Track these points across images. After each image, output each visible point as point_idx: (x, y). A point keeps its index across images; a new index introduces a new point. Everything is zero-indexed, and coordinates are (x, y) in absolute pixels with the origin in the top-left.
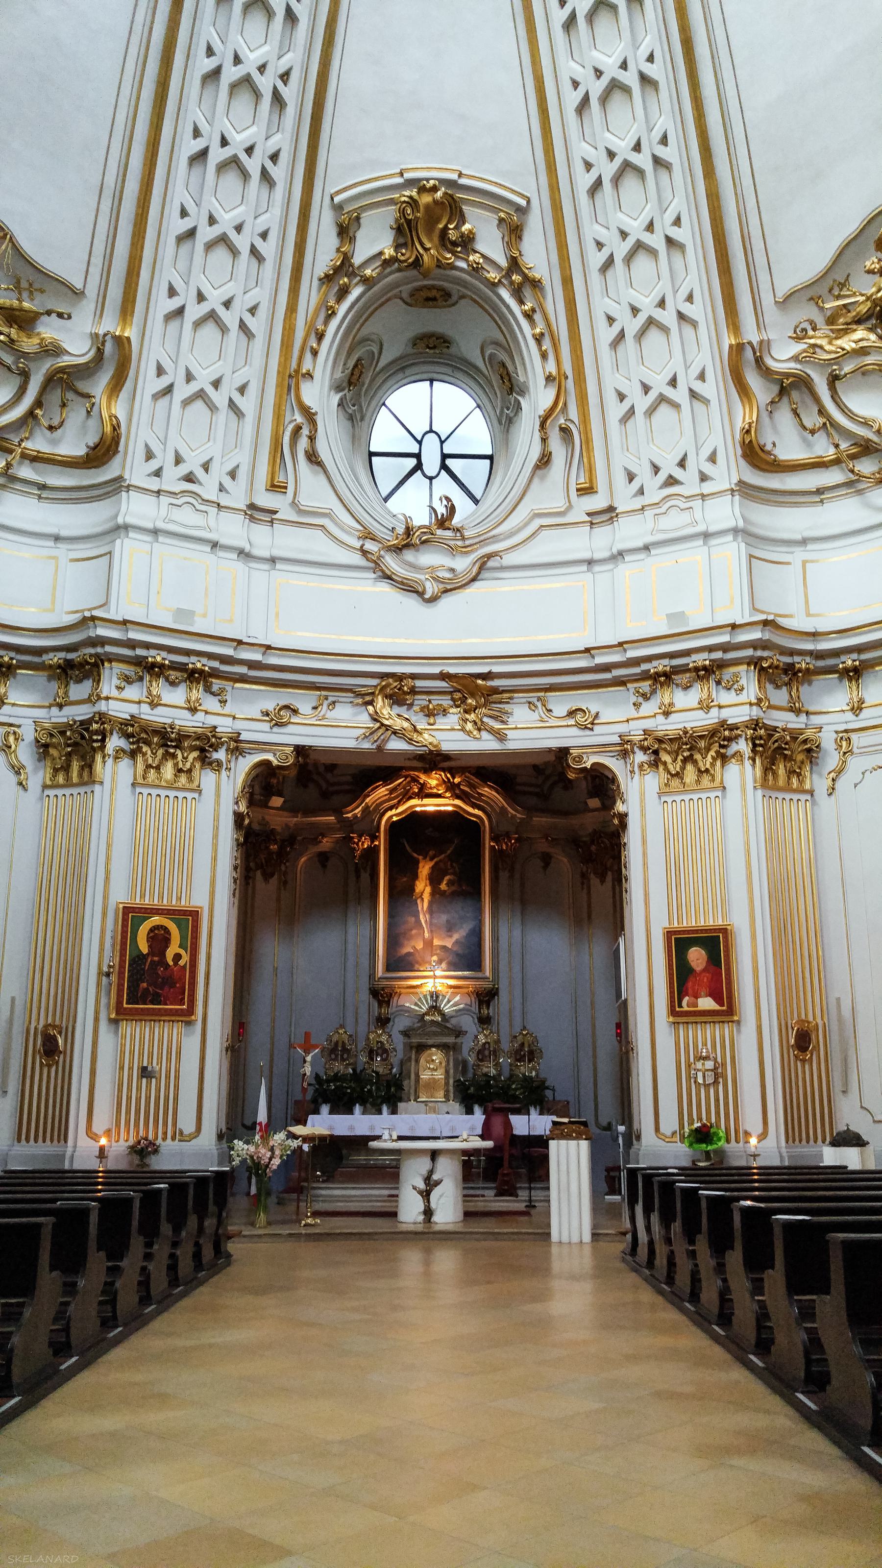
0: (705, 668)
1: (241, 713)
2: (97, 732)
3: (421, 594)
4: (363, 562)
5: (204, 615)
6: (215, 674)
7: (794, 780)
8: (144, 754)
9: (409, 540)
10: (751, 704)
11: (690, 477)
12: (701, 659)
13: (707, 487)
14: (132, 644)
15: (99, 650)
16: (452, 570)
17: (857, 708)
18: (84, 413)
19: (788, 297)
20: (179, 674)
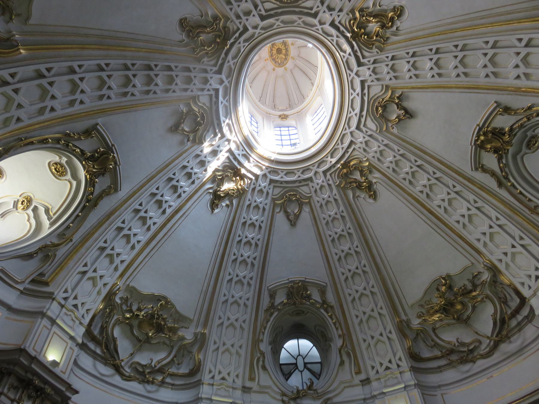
18: (189, 358)
19: (412, 306)
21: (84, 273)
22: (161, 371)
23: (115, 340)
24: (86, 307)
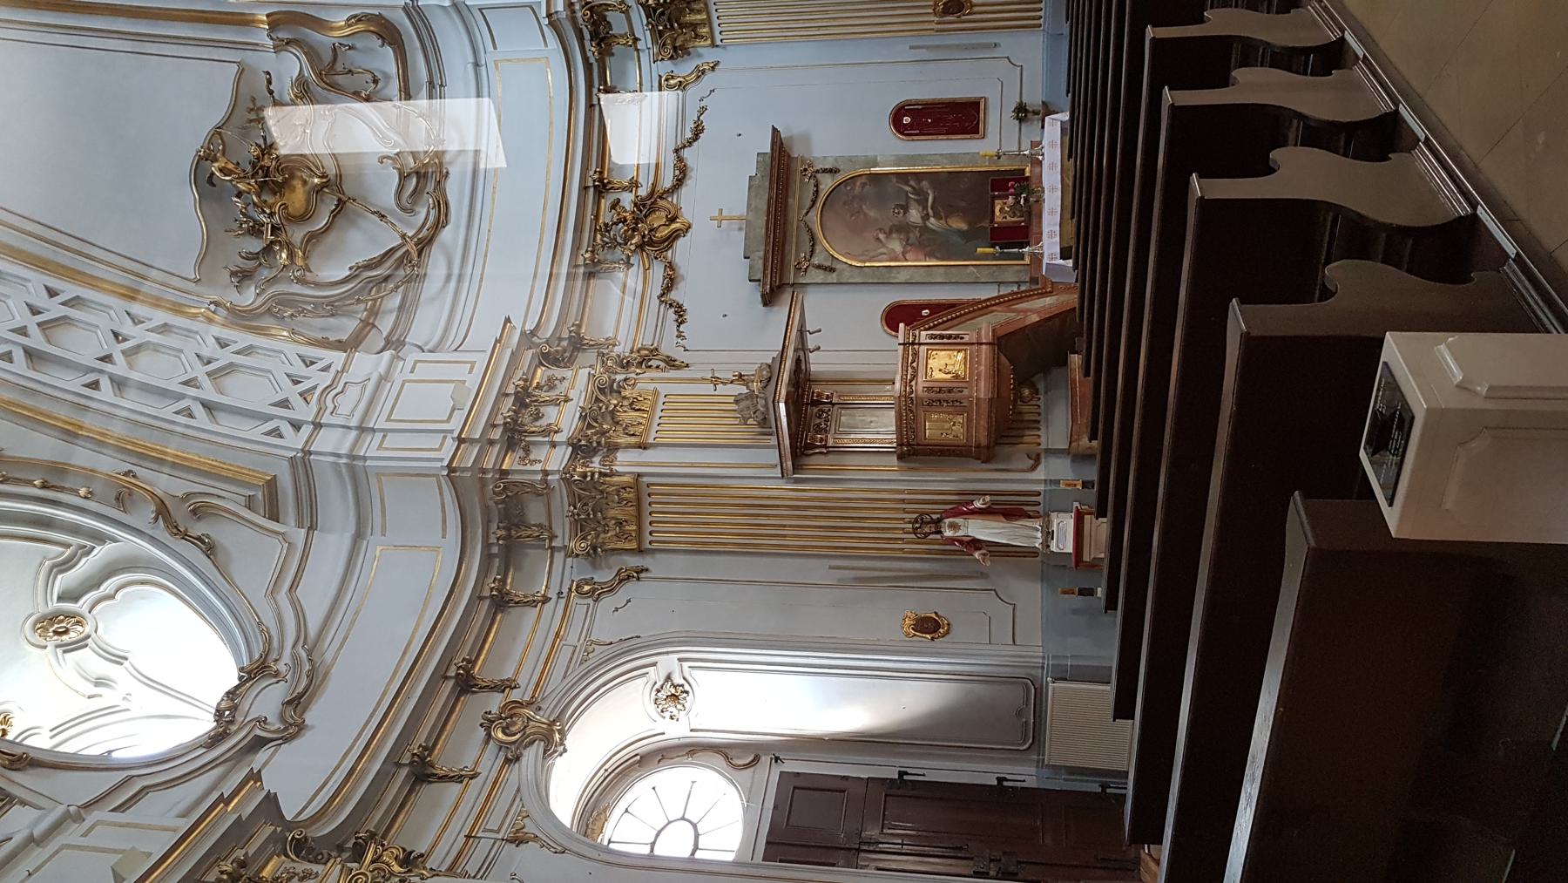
21: (208, 407)
24: (299, 369)
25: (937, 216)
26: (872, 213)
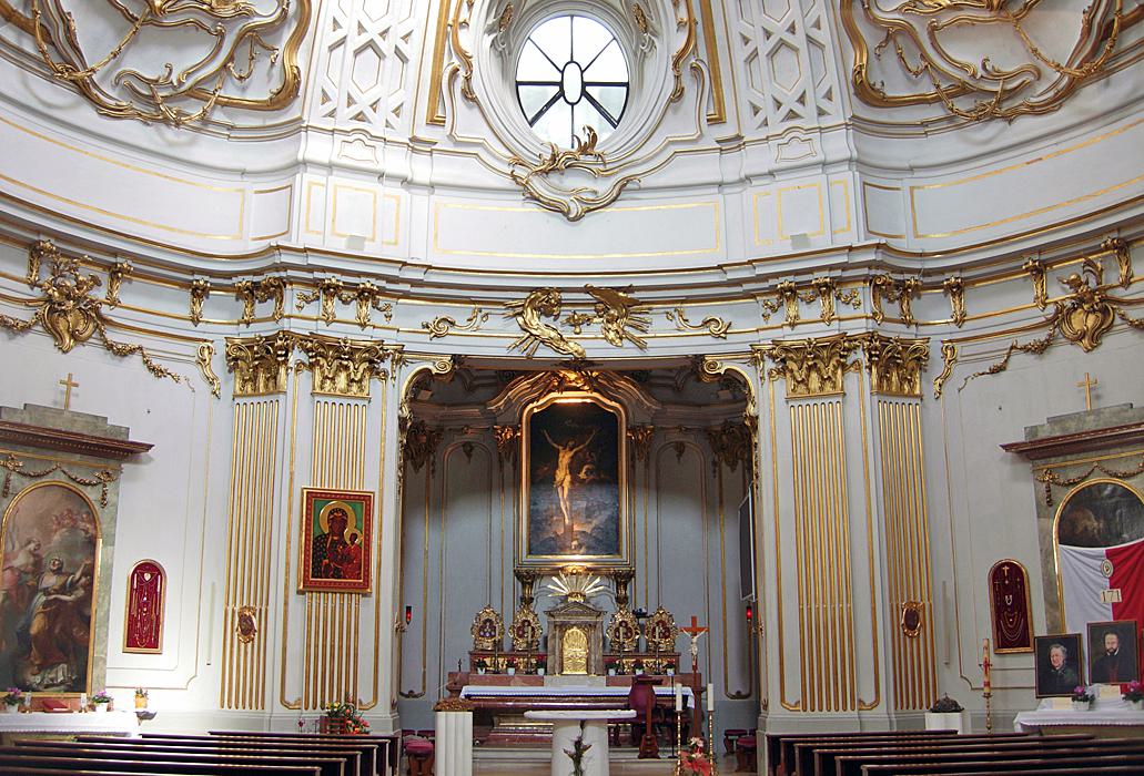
0: (826, 285)
1: (403, 326)
2: (280, 348)
3: (566, 214)
4: (514, 186)
5: (373, 240)
6: (382, 292)
7: (906, 387)
8: (322, 367)
9: (555, 165)
10: (867, 318)
11: (808, 112)
12: (821, 277)
13: (825, 122)
14: (311, 269)
15: (283, 274)
16: (595, 192)
17: (960, 322)
20: (350, 293)
22: (195, 93)
23: (65, 19)
25: (47, 604)
26: (56, 537)
